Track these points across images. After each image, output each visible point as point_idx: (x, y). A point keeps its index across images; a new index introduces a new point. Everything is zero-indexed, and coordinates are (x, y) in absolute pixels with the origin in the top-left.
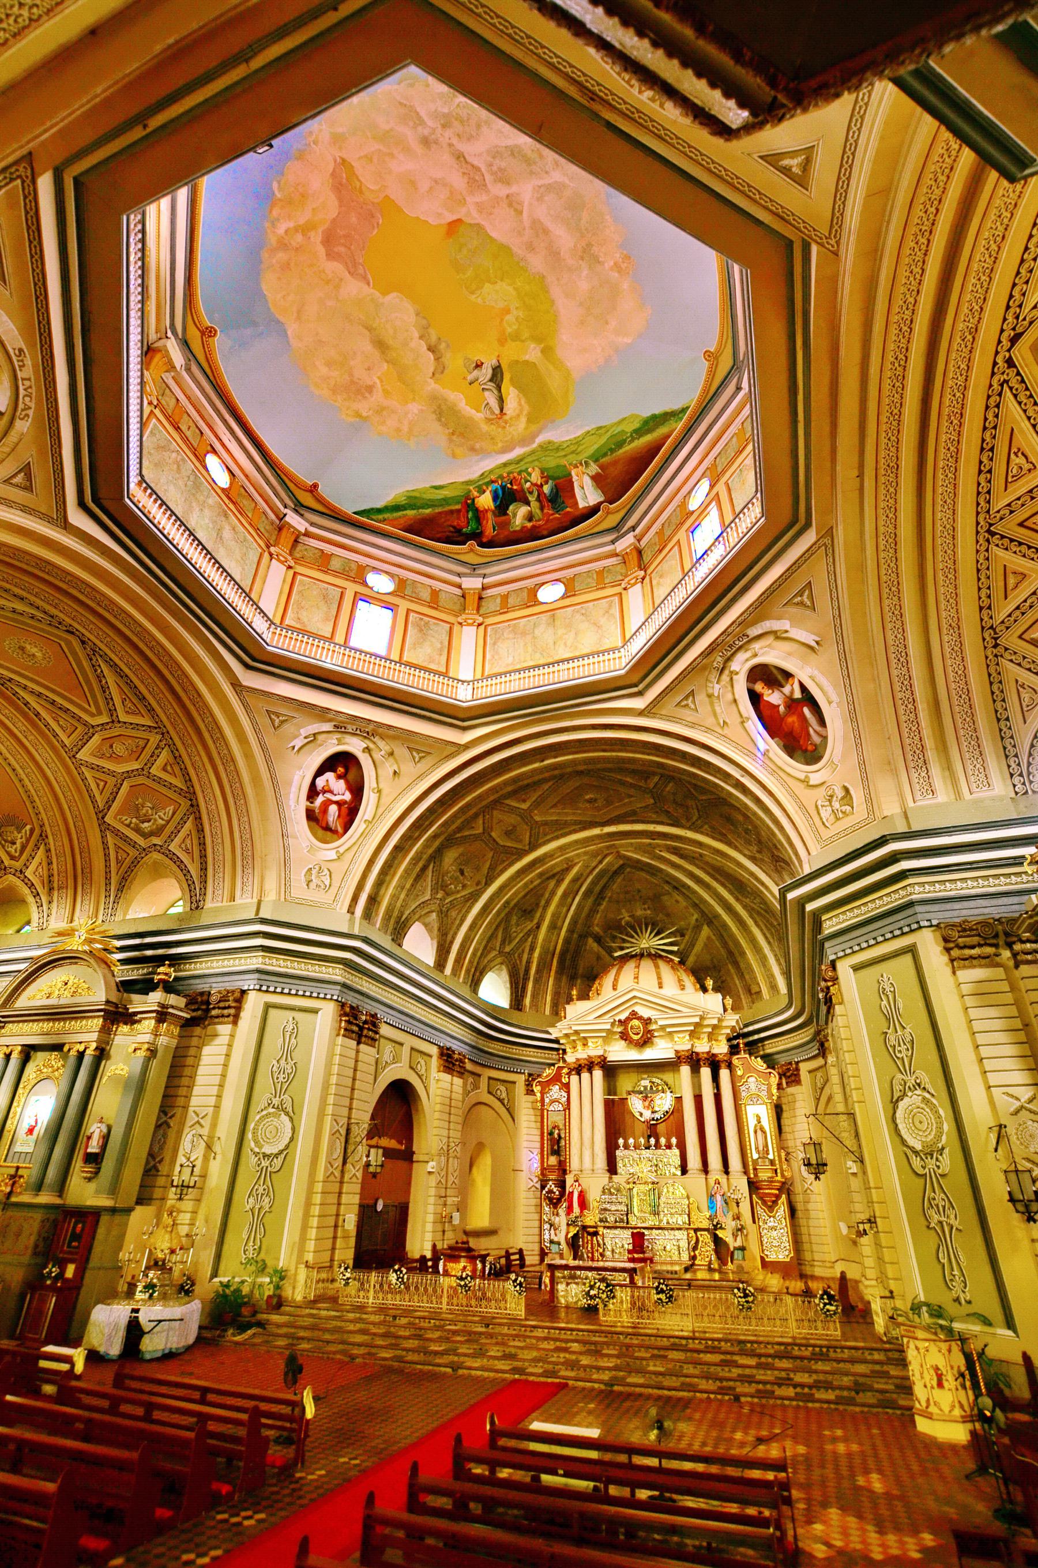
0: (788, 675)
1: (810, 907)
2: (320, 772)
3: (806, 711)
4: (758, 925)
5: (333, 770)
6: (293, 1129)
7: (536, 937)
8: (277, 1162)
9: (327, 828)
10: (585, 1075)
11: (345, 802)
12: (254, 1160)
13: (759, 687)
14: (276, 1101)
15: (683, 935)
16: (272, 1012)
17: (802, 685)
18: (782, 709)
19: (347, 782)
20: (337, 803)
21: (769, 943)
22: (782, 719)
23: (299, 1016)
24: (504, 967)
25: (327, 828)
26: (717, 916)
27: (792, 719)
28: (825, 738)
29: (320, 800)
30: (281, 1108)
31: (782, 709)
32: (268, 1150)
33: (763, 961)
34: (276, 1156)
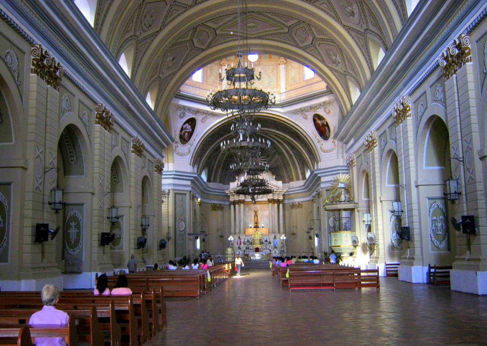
0: (324, 119)
1: (319, 175)
2: (185, 124)
3: (326, 128)
4: (296, 158)
5: (188, 123)
6: (186, 225)
7: (217, 157)
8: (183, 232)
9: (184, 140)
10: (237, 206)
11: (189, 132)
12: (178, 232)
13: (316, 118)
14: (181, 218)
15: (268, 157)
16: (177, 196)
17: (327, 123)
18: (321, 125)
19: (191, 126)
20: (188, 132)
21: (299, 164)
22: (320, 127)
23: (183, 196)
24: (207, 168)
25: (184, 140)
26: (283, 153)
27: (322, 128)
28: (329, 136)
29: (183, 132)
30: (182, 220)
31: (321, 125)
32: (181, 230)
33: (296, 169)
34: (183, 231)
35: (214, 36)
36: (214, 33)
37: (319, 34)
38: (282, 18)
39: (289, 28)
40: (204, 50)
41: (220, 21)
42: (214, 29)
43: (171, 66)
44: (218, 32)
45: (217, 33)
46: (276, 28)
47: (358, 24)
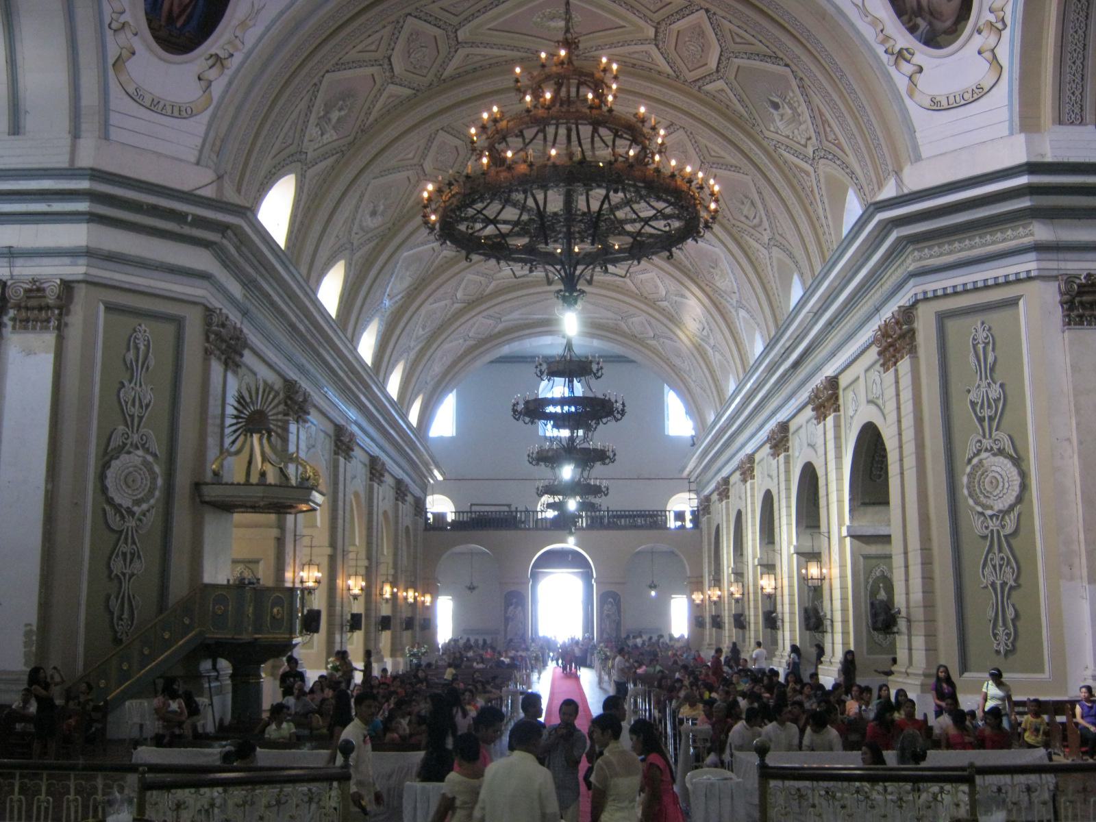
35: (663, 24)
36: (661, 36)
37: (389, 98)
38: (479, 57)
39: (458, 43)
40: (707, 11)
41: (636, 56)
42: (657, 46)
43: (790, 104)
44: (651, 32)
45: (653, 30)
46: (491, 25)
47: (362, 229)
